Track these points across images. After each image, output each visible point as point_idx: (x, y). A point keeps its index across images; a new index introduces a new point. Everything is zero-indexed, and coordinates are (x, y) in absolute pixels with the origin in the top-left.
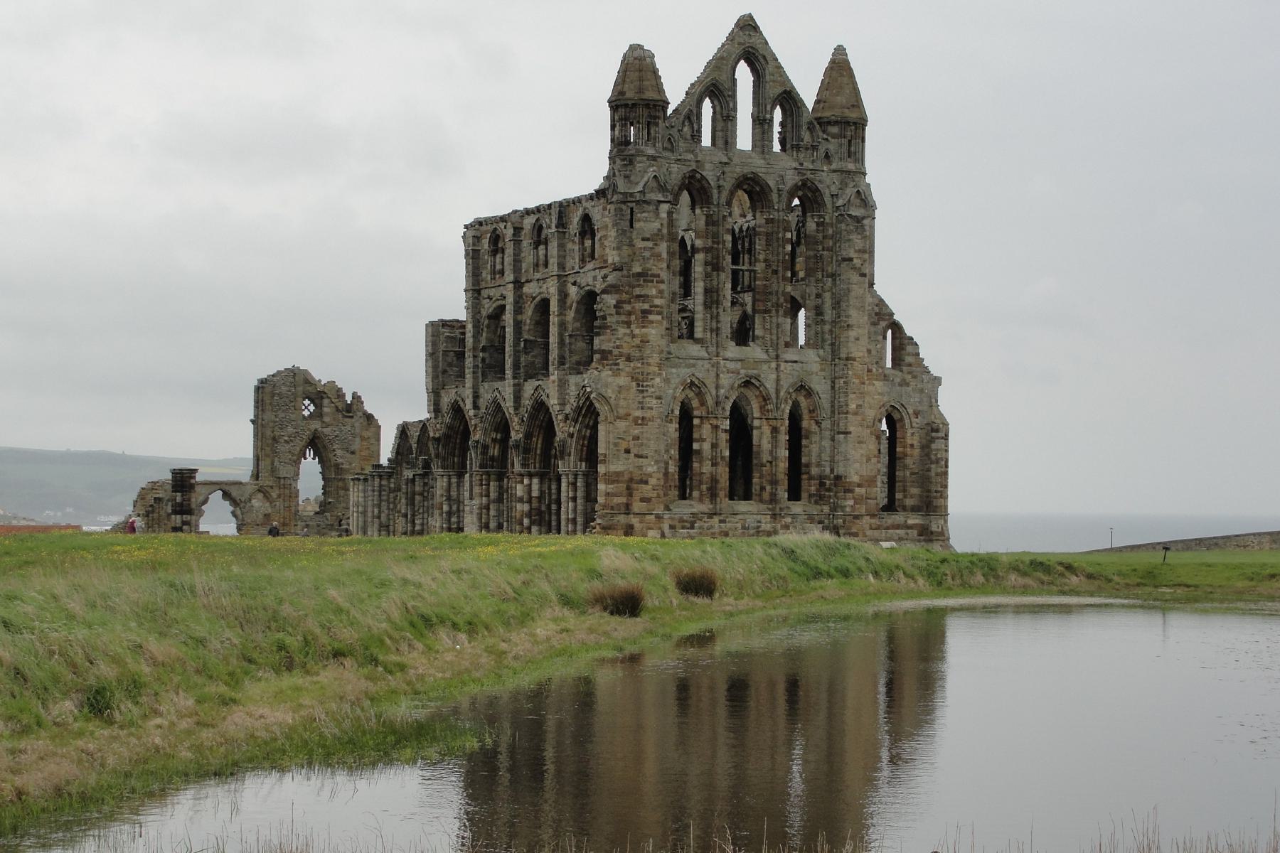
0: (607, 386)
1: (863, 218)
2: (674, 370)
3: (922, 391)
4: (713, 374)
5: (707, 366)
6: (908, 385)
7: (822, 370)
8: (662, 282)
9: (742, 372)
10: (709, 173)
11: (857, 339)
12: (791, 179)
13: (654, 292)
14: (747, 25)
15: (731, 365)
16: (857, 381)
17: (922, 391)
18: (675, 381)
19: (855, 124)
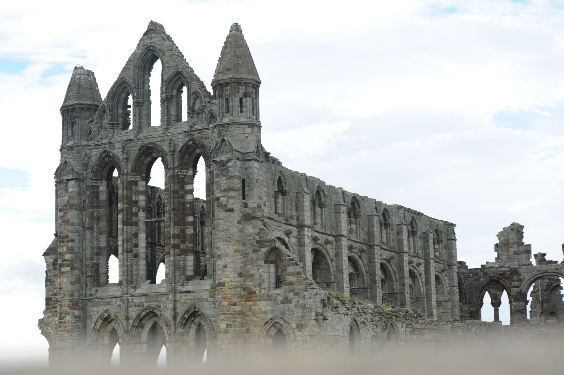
0: (48, 324)
1: (228, 161)
2: (95, 309)
3: (304, 306)
4: (123, 308)
5: (119, 302)
6: (290, 302)
7: (211, 297)
8: (73, 241)
9: (146, 304)
10: (117, 151)
11: (225, 267)
12: (181, 141)
13: (65, 249)
14: (154, 29)
15: (137, 300)
16: (225, 303)
17: (304, 306)
18: (96, 317)
19: (227, 84)
